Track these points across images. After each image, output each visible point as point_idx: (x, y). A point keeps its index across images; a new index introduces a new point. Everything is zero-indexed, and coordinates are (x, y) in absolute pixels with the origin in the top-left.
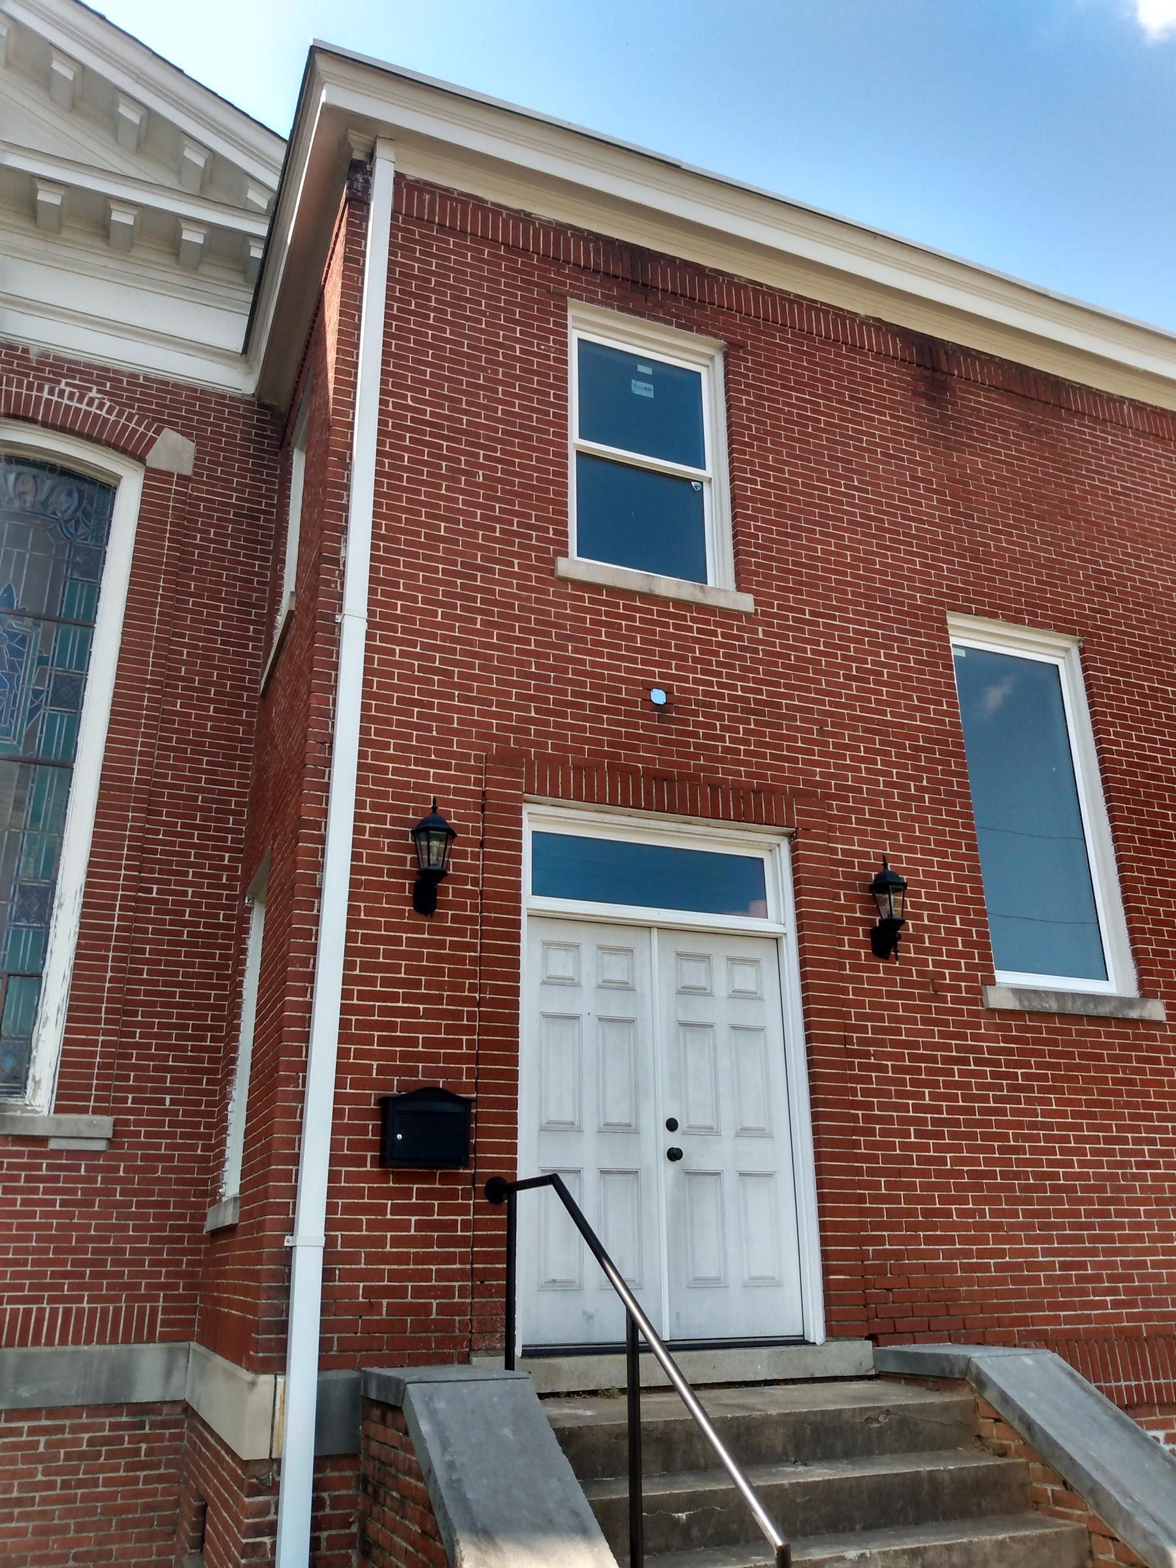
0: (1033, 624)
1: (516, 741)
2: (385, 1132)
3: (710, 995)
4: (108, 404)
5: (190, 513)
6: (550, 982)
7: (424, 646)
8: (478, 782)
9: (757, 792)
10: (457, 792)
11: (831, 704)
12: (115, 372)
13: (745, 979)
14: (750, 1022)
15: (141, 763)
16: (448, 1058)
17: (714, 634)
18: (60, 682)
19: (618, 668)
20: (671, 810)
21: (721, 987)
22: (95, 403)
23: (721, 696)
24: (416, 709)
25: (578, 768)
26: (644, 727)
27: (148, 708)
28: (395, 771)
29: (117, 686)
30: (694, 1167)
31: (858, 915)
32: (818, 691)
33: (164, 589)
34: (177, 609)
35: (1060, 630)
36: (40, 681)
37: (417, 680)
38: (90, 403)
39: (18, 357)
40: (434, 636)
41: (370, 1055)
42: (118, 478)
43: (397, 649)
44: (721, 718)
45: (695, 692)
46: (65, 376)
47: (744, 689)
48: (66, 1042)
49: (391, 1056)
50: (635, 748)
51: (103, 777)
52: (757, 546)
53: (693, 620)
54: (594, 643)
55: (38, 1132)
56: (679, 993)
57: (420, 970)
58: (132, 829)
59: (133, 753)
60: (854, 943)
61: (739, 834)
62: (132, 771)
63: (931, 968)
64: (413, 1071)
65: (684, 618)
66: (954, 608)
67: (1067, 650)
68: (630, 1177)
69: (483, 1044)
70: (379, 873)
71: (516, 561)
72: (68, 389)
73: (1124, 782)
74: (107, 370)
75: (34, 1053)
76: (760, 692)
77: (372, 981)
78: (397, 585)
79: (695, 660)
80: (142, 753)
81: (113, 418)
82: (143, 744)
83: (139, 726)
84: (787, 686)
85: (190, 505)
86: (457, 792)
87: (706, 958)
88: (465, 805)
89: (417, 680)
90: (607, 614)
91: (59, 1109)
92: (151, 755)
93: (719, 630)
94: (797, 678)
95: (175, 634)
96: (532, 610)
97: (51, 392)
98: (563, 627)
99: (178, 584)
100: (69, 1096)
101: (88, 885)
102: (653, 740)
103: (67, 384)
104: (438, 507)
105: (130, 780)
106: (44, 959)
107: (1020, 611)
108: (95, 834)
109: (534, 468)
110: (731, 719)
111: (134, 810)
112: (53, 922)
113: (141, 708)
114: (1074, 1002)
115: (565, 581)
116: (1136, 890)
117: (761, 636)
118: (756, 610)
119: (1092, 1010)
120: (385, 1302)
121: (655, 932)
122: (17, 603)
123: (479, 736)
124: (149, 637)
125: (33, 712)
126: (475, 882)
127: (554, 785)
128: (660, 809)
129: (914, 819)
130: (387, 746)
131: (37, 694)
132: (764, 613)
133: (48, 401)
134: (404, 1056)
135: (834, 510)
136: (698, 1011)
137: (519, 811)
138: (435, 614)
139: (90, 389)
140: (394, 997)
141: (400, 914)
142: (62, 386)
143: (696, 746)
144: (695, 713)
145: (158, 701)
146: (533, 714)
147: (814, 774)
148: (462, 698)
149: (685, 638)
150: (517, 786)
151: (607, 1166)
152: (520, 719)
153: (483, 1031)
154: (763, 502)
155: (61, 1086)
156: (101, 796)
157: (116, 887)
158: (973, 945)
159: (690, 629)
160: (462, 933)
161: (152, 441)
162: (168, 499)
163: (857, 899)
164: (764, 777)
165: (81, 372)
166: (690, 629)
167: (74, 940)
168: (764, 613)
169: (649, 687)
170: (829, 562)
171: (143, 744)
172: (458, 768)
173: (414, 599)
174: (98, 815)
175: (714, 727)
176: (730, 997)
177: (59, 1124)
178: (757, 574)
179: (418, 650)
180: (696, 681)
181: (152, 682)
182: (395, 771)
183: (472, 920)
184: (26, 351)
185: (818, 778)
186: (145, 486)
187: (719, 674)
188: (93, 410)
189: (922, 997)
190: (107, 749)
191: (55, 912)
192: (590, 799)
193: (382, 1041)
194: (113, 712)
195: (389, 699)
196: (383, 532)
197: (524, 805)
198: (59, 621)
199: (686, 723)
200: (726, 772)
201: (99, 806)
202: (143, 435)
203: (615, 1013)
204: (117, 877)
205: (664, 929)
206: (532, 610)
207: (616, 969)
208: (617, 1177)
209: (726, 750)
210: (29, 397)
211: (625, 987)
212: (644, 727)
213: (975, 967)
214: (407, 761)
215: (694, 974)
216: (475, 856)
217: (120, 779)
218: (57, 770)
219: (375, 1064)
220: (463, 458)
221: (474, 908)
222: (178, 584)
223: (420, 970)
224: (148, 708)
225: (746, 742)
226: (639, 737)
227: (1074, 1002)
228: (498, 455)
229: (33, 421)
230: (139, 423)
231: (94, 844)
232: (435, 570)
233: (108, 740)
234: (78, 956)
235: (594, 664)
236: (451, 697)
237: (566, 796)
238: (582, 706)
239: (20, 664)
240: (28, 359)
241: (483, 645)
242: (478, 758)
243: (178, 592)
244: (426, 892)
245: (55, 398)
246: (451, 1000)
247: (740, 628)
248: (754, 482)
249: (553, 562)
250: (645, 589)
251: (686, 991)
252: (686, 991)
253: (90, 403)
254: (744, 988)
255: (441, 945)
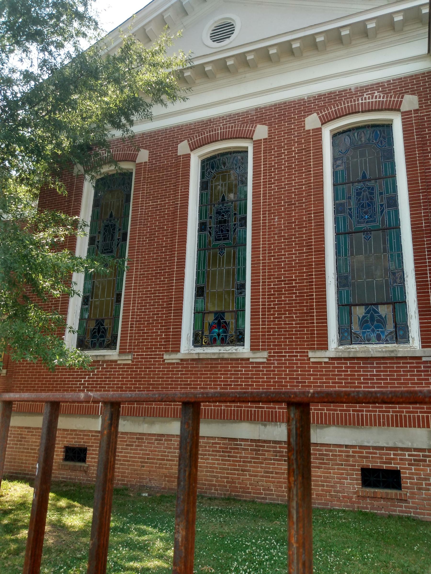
4: (382, 95)
5: (421, 122)
12: (382, 83)
15: (425, 220)
18: (389, 199)
22: (379, 97)
27: (423, 199)
29: (409, 194)
33: (419, 154)
34: (425, 160)
36: (382, 201)
38: (376, 98)
39: (348, 93)
42: (392, 120)
46: (365, 92)
48: (421, 323)
51: (412, 228)
55: (417, 355)
58: (427, 244)
59: (421, 217)
62: (422, 223)
72: (367, 96)
74: (379, 83)
75: (410, 328)
80: (424, 216)
81: (385, 100)
82: (424, 213)
83: (421, 206)
85: (421, 119)
91: (423, 347)
92: (428, 216)
95: (426, 169)
97: (362, 100)
99: (423, 150)
100: (426, 342)
101: (416, 267)
103: (367, 95)
105: (422, 227)
106: (406, 296)
108: (414, 249)
111: (426, 237)
112: (406, 283)
113: (420, 200)
122: (368, 177)
124: (417, 173)
125: (382, 212)
131: (382, 205)
133: (362, 103)
139: (375, 93)
142: (365, 96)
145: (426, 195)
155: (422, 339)
156: (413, 235)
157: (426, 266)
161: (401, 102)
162: (412, 121)
165: (370, 88)
167: (415, 288)
171: (424, 213)
174: (413, 242)
177: (424, 352)
181: (422, 189)
184: (350, 89)
186: (402, 119)
188: (378, 99)
190: (411, 218)
191: (406, 279)
194: (410, 204)
198: (383, 178)
201: (413, 239)
202: (397, 101)
204: (426, 263)
210: (355, 105)
217: (419, 227)
218: (395, 230)
222: (423, 150)
224: (423, 199)
229: (359, 112)
230: (395, 98)
231: (414, 253)
233: (411, 214)
234: (418, 293)
239: (374, 197)
240: (352, 92)
243: (424, 153)
245: (364, 101)
253: (376, 98)
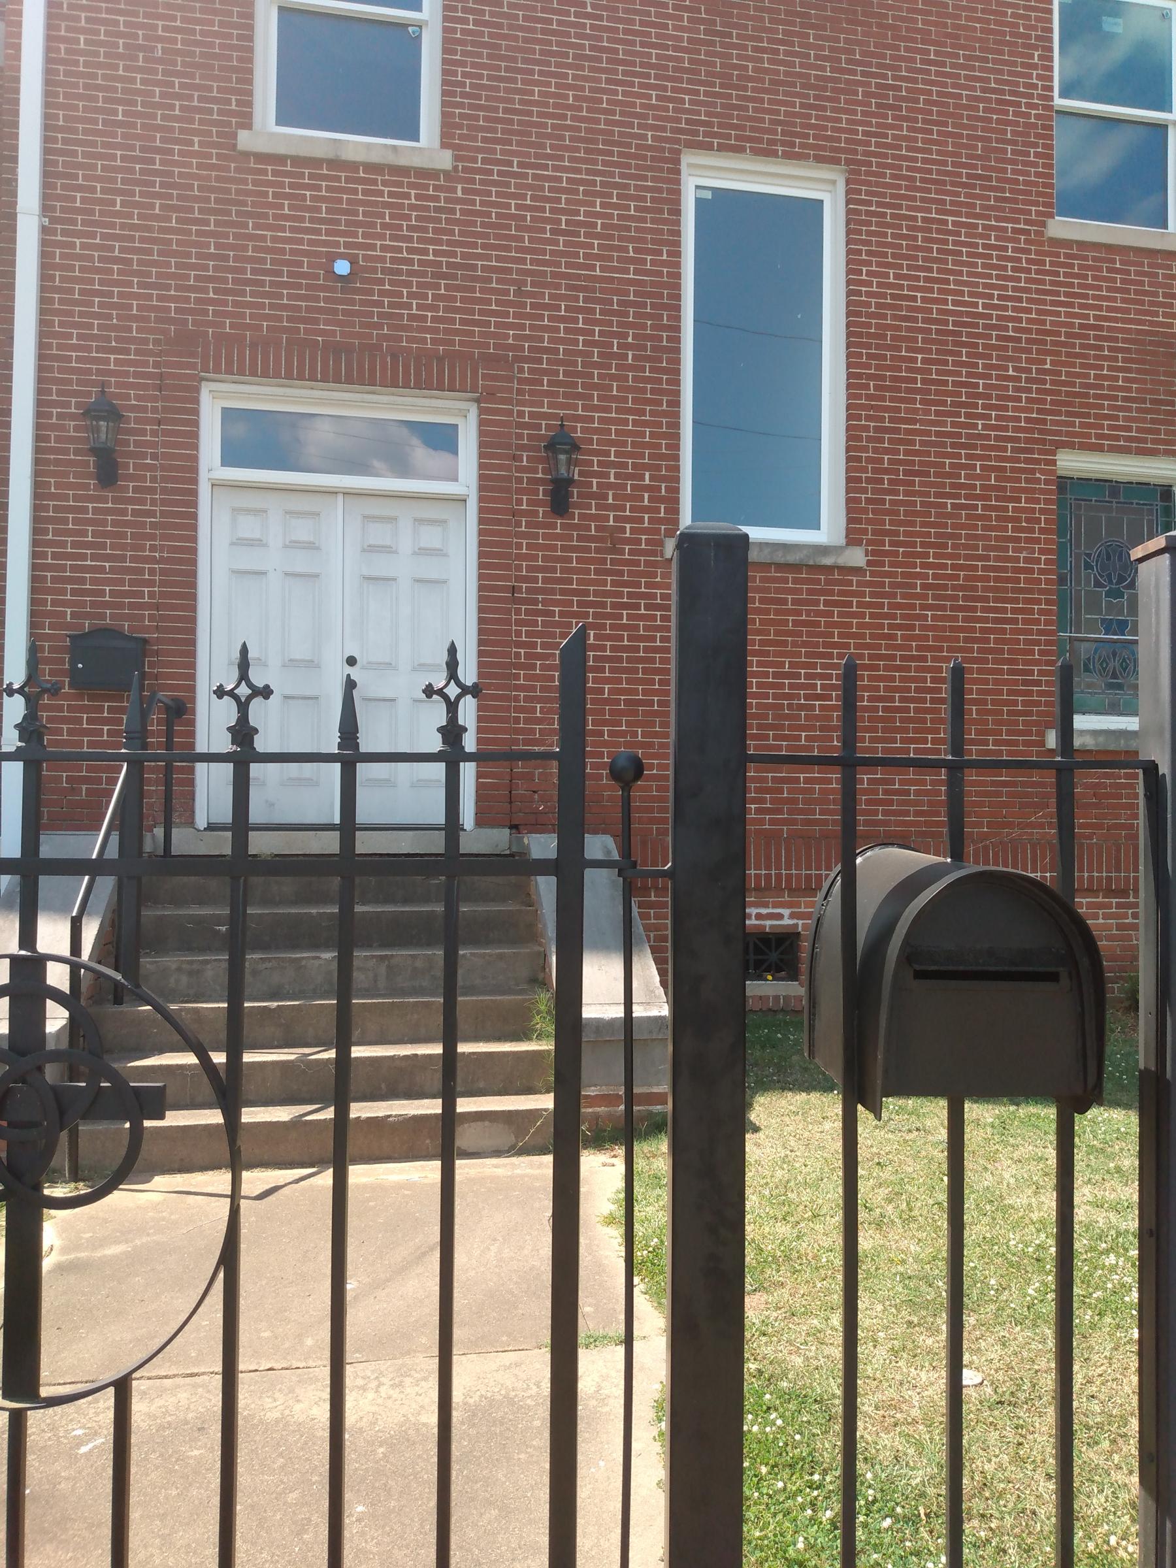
0: (788, 156)
1: (195, 322)
2: (73, 663)
3: (396, 552)
6: (239, 543)
7: (104, 237)
8: (157, 365)
9: (440, 360)
10: (136, 375)
11: (532, 262)
13: (431, 537)
14: (434, 575)
16: (132, 606)
17: (407, 196)
19: (300, 241)
20: (349, 380)
21: (406, 544)
23: (410, 262)
24: (97, 300)
25: (254, 345)
26: (326, 299)
28: (79, 359)
30: (372, 695)
31: (540, 475)
32: (519, 250)
35: (819, 159)
37: (98, 271)
40: (112, 225)
41: (65, 603)
43: (78, 241)
44: (408, 284)
45: (382, 259)
47: (436, 253)
49: (83, 604)
50: (316, 321)
52: (464, 95)
53: (384, 183)
54: (276, 217)
56: (364, 550)
57: (105, 534)
60: (532, 502)
61: (427, 402)
63: (611, 523)
64: (102, 616)
65: (375, 182)
66: (691, 145)
67: (834, 182)
68: (310, 702)
69: (163, 595)
70: (65, 452)
71: (196, 139)
73: (869, 325)
76: (454, 255)
77: (63, 544)
78: (76, 177)
79: (385, 226)
84: (484, 246)
86: (136, 375)
87: (393, 520)
88: (144, 387)
89: (98, 271)
90: (291, 186)
93: (413, 192)
94: (497, 236)
96: (212, 190)
98: (244, 204)
102: (335, 312)
104: (115, 90)
107: (772, 142)
109: (216, 35)
110: (419, 285)
114: (761, 550)
115: (246, 155)
116: (860, 439)
117: (459, 194)
118: (455, 168)
119: (779, 558)
120: (84, 787)
121: (340, 497)
123: (158, 320)
126: (154, 457)
127: (229, 363)
128: (337, 380)
129: (613, 377)
130: (69, 336)
132: (465, 170)
134: (93, 604)
135: (558, 44)
136: (381, 566)
137: (197, 390)
138: (114, 203)
140: (83, 557)
141: (86, 487)
143: (380, 315)
144: (381, 282)
146: (211, 295)
147: (507, 336)
148: (141, 285)
149: (376, 204)
150: (193, 366)
151: (289, 692)
152: (198, 301)
153: (163, 584)
154: (474, 44)
158: (662, 500)
159: (381, 193)
160: (142, 502)
163: (539, 460)
164: (452, 343)
166: (381, 193)
168: (465, 170)
169: (332, 258)
170: (547, 105)
172: (138, 352)
173: (93, 190)
175: (401, 295)
176: (414, 553)
178: (460, 127)
179: (98, 241)
180: (384, 248)
182: (79, 359)
183: (152, 490)
185: (510, 341)
187: (409, 239)
189: (598, 550)
192: (265, 375)
193: (74, 592)
195: (71, 291)
196: (61, 123)
197: (204, 383)
199: (370, 292)
200: (410, 340)
203: (299, 569)
205: (348, 493)
206: (212, 190)
207: (302, 530)
208: (300, 701)
209: (412, 317)
211: (311, 546)
212: (326, 299)
213: (661, 521)
214: (88, 349)
215: (379, 534)
216: (154, 433)
219: (69, 611)
220: (140, 33)
221: (154, 479)
223: (105, 534)
225: (435, 308)
226: (320, 310)
227: (761, 550)
228: (178, 23)
232: (113, 157)
235: (275, 239)
236: (130, 284)
237: (241, 372)
238: (262, 283)
241: (162, 230)
242: (157, 342)
244: (108, 470)
246: (134, 559)
247: (436, 188)
248: (465, 21)
249: (234, 136)
250: (331, 156)
251: (371, 549)
252: (371, 549)
254: (429, 546)
255: (123, 512)
